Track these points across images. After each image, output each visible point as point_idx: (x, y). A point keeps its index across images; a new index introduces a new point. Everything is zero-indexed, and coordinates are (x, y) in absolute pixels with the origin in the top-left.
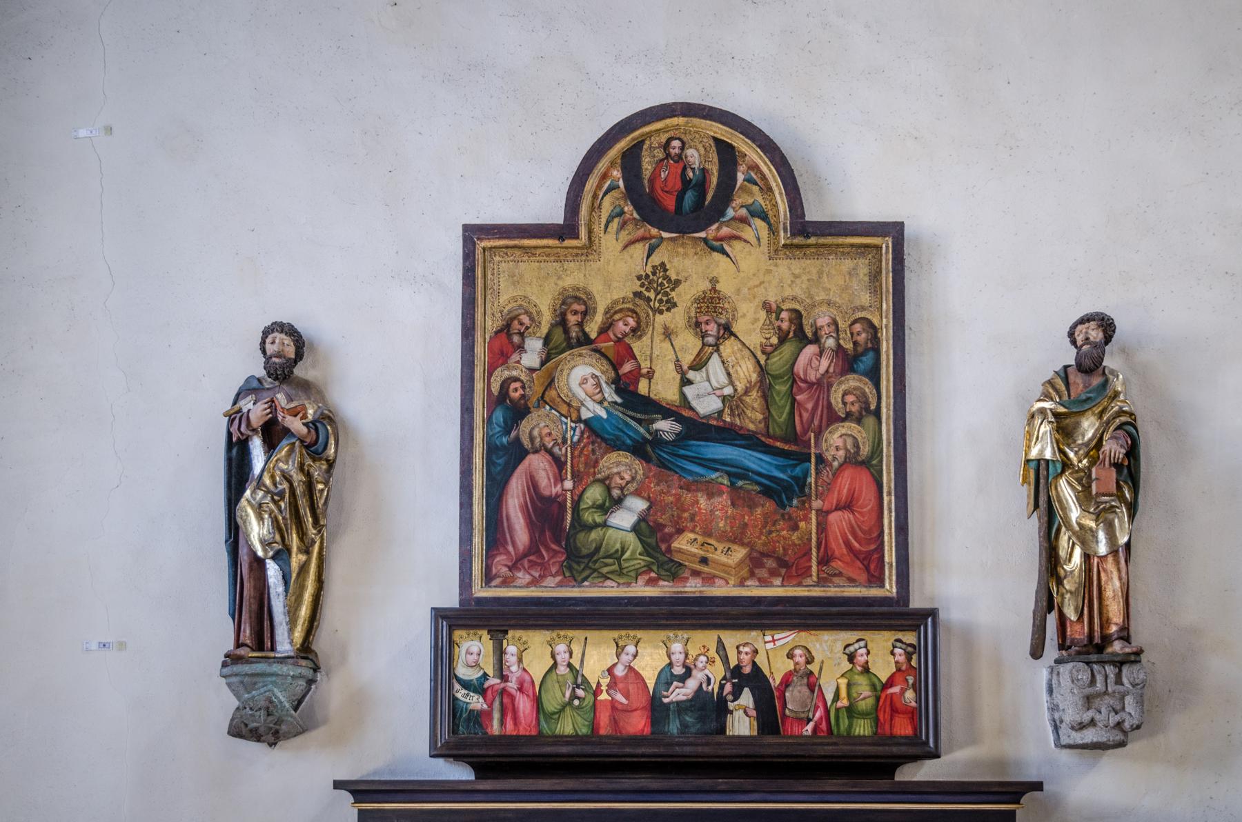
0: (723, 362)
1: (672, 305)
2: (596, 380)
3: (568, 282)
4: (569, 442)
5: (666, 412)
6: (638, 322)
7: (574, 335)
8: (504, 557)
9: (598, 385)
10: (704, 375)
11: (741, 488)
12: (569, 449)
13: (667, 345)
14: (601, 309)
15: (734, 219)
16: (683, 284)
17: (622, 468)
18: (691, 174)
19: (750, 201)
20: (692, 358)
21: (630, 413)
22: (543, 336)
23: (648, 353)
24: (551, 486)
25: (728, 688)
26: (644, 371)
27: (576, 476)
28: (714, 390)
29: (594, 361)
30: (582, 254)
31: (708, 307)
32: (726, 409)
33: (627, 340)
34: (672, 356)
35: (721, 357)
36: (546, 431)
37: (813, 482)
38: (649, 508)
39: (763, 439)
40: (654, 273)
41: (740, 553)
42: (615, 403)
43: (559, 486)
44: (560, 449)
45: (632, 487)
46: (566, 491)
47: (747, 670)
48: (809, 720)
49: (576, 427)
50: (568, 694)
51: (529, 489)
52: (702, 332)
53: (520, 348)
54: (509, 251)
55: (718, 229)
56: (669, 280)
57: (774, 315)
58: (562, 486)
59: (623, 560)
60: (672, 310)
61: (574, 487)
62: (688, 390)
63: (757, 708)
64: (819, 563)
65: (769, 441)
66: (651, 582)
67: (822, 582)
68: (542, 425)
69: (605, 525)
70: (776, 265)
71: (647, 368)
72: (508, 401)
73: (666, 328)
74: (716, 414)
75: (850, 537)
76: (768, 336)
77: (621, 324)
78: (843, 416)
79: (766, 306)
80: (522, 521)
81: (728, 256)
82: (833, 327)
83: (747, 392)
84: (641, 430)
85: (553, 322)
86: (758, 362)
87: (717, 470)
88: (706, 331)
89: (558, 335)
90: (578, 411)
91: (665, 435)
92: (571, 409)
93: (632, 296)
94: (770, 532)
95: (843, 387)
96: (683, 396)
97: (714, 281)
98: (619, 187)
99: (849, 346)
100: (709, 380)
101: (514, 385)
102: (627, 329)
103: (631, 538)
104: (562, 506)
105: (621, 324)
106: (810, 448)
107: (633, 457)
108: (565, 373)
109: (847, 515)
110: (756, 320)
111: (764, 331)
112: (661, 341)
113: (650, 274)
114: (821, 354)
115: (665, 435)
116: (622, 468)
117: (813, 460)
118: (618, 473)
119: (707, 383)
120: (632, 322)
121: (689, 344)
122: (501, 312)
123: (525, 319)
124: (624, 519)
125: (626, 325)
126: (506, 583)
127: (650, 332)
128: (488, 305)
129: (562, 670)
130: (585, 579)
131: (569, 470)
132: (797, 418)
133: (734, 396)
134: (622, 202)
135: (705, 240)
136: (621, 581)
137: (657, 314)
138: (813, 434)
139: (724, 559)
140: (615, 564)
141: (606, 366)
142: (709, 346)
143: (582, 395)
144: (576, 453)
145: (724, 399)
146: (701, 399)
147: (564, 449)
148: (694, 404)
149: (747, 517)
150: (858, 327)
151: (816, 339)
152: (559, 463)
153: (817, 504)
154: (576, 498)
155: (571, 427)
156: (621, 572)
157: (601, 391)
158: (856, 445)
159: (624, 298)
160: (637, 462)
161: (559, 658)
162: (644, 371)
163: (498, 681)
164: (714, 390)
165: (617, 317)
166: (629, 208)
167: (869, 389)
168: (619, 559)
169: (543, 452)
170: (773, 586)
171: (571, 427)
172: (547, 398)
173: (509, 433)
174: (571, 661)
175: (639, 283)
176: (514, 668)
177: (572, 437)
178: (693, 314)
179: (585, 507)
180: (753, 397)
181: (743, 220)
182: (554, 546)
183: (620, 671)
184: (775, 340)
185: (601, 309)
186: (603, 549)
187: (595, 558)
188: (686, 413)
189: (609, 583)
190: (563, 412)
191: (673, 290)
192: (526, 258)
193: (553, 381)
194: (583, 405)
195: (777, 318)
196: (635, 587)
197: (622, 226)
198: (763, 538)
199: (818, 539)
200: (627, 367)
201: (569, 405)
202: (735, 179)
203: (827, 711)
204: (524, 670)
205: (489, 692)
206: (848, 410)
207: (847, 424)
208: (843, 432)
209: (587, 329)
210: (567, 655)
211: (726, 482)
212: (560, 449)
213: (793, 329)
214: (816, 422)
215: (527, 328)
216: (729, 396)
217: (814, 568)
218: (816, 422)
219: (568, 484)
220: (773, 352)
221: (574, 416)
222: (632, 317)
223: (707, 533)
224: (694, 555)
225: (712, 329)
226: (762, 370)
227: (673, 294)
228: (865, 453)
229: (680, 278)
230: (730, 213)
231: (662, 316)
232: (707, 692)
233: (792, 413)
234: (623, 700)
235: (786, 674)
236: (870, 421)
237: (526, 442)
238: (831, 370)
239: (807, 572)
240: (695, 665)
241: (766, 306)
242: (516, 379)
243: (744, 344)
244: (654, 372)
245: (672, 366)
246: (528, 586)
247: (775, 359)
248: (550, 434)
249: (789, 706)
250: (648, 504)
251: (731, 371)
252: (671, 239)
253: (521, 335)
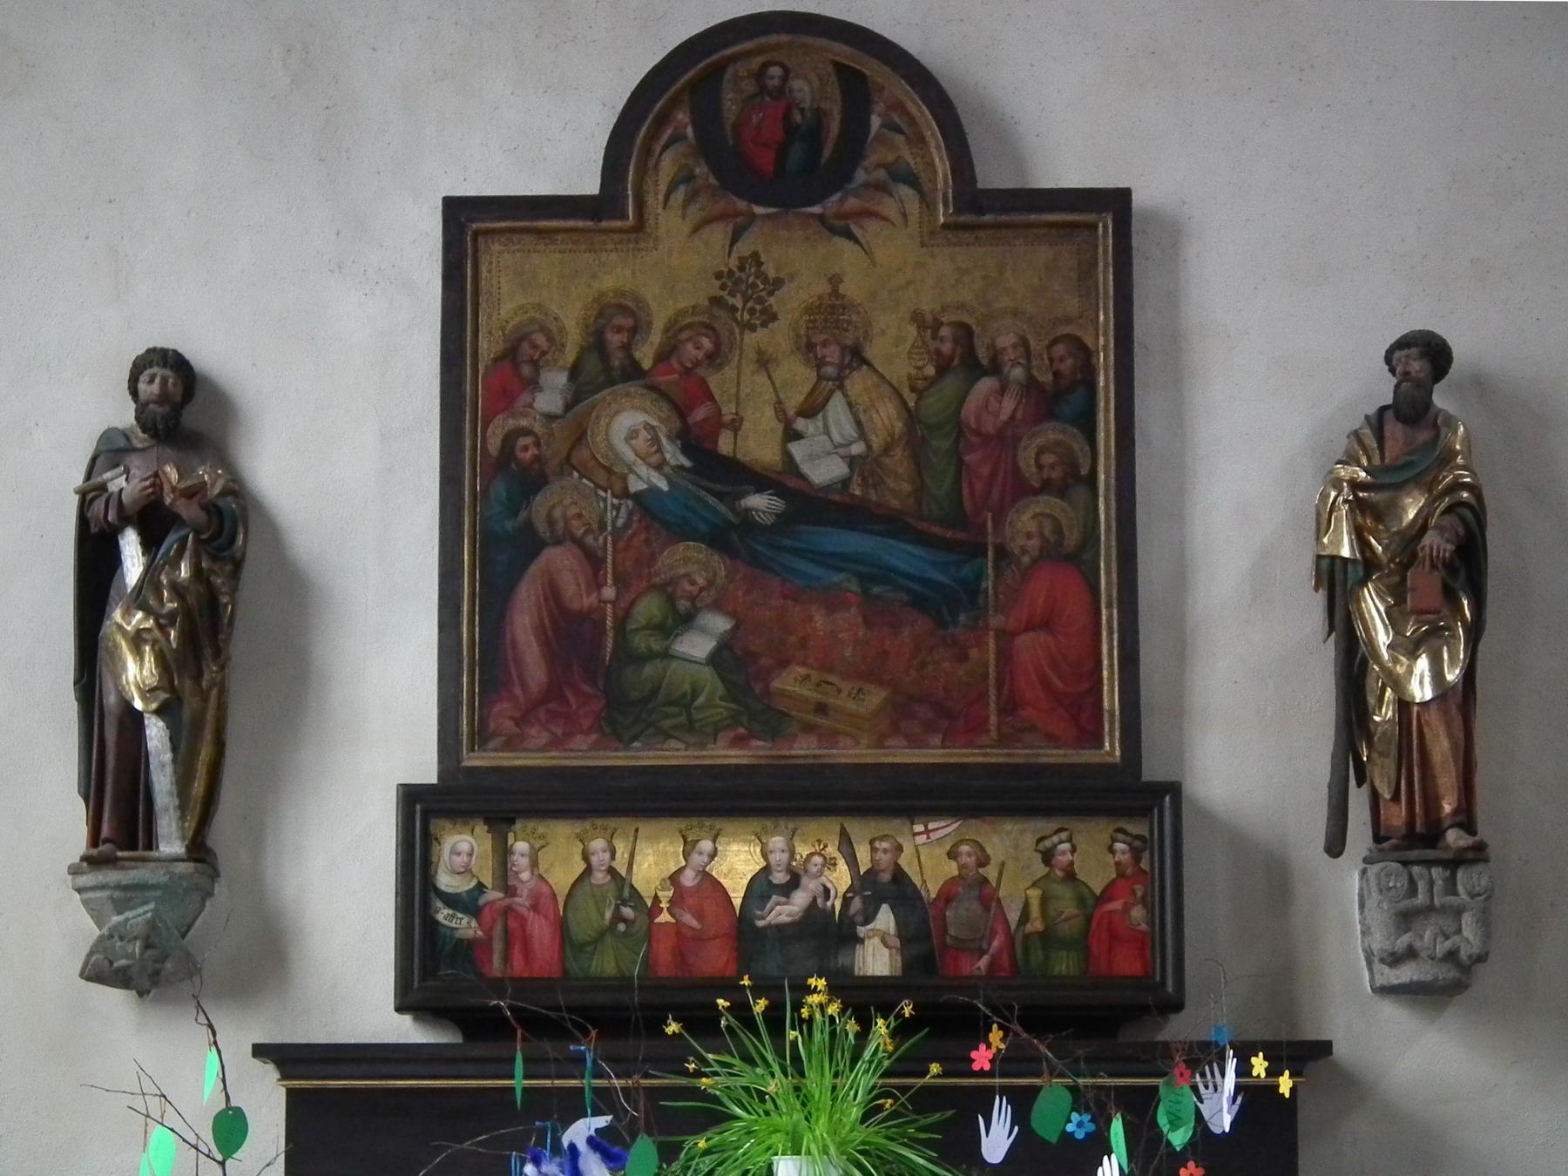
0: (850, 405)
1: (770, 317)
2: (651, 431)
3: (608, 283)
4: (609, 528)
5: (760, 481)
6: (717, 344)
7: (616, 363)
8: (506, 705)
9: (655, 440)
10: (820, 424)
11: (878, 597)
12: (609, 538)
13: (762, 379)
14: (659, 324)
15: (866, 185)
16: (787, 283)
17: (691, 568)
18: (798, 118)
19: (891, 157)
20: (802, 398)
21: (706, 483)
22: (569, 366)
23: (733, 391)
24: (581, 596)
25: (857, 904)
26: (727, 418)
27: (621, 581)
28: (835, 447)
29: (649, 403)
30: (630, 240)
31: (826, 321)
32: (856, 477)
33: (701, 372)
34: (769, 395)
35: (845, 395)
36: (573, 511)
37: (990, 588)
38: (735, 628)
39: (912, 521)
40: (741, 268)
41: (876, 697)
42: (682, 467)
43: (595, 595)
44: (596, 539)
45: (708, 597)
46: (605, 602)
47: (886, 877)
48: (982, 953)
49: (620, 504)
50: (608, 915)
51: (546, 599)
52: (816, 358)
53: (533, 385)
54: (515, 237)
55: (842, 200)
56: (766, 280)
57: (929, 332)
58: (599, 594)
59: (695, 708)
60: (770, 325)
61: (617, 597)
62: (796, 449)
63: (900, 935)
64: (1001, 712)
65: (923, 526)
66: (739, 742)
67: (1004, 740)
68: (567, 501)
69: (667, 655)
70: (932, 256)
71: (732, 413)
72: (513, 466)
73: (760, 352)
74: (839, 485)
75: (1049, 672)
76: (920, 364)
77: (690, 347)
78: (1037, 485)
79: (917, 318)
80: (535, 648)
81: (856, 241)
82: (1021, 349)
83: (887, 450)
84: (723, 508)
85: (583, 343)
86: (904, 403)
87: (840, 570)
88: (824, 357)
89: (593, 364)
90: (624, 479)
91: (759, 516)
92: (612, 476)
93: (706, 303)
94: (924, 664)
95: (1038, 441)
96: (788, 457)
97: (835, 280)
98: (685, 138)
99: (1046, 378)
100: (827, 432)
101: (522, 441)
102: (700, 355)
103: (707, 673)
104: (599, 626)
105: (690, 347)
106: (986, 536)
107: (710, 551)
108: (603, 422)
109: (1043, 637)
110: (898, 341)
111: (914, 356)
112: (753, 373)
113: (735, 270)
114: (1002, 390)
115: (759, 516)
116: (691, 568)
117: (990, 554)
118: (687, 575)
119: (826, 437)
120: (706, 343)
121: (797, 377)
122: (503, 329)
123: (540, 340)
124: (697, 646)
125: (698, 348)
126: (510, 744)
127: (736, 359)
128: (482, 319)
129: (600, 877)
130: (635, 738)
131: (609, 570)
132: (966, 492)
133: (867, 456)
134: (690, 162)
135: (821, 218)
136: (692, 740)
137: (747, 332)
138: (990, 514)
139: (851, 705)
140: (680, 715)
141: (665, 410)
142: (829, 379)
143: (629, 455)
144: (621, 544)
145: (852, 461)
146: (817, 462)
147: (601, 538)
148: (805, 468)
149: (887, 642)
150: (1060, 349)
151: (995, 368)
152: (594, 560)
153: (996, 621)
154: (620, 613)
155: (613, 505)
156: (690, 727)
157: (660, 450)
158: (1058, 529)
159: (694, 307)
160: (716, 557)
161: (594, 860)
162: (727, 418)
163: (501, 895)
164: (835, 447)
165: (683, 336)
166: (701, 170)
167: (1079, 445)
168: (688, 707)
169: (568, 543)
170: (927, 746)
171: (613, 505)
172: (574, 461)
173: (516, 514)
174: (614, 864)
175: (717, 283)
176: (525, 876)
177: (614, 521)
178: (802, 332)
179: (634, 627)
180: (896, 458)
181: (880, 187)
182: (587, 688)
183: (689, 879)
184: (930, 371)
185: (659, 324)
186: (662, 691)
187: (651, 706)
188: (792, 483)
189: (673, 743)
190: (601, 483)
191: (771, 293)
192: (541, 247)
193: (584, 433)
194: (632, 471)
195: (935, 337)
196: (713, 749)
197: (691, 198)
198: (913, 673)
199: (998, 673)
200: (700, 413)
201: (609, 471)
202: (866, 125)
203: (1010, 938)
204: (541, 878)
205: (487, 911)
206: (1045, 476)
207: (1043, 498)
208: (1037, 510)
209: (637, 355)
210: (607, 855)
211: (854, 586)
212: (596, 539)
213: (958, 353)
214: (996, 494)
215: (544, 353)
216: (860, 456)
217: (993, 719)
218: (996, 494)
219: (609, 592)
220: (927, 389)
221: (618, 488)
222: (707, 336)
223: (826, 666)
224: (806, 700)
225: (832, 354)
226: (911, 417)
227: (772, 300)
228: (1073, 543)
229: (781, 275)
230: (860, 176)
231: (754, 335)
232: (824, 911)
233: (958, 481)
234: (694, 923)
235: (946, 883)
236: (1080, 493)
237: (542, 527)
238: (1019, 415)
239: (980, 726)
240: (806, 871)
241: (917, 318)
242: (527, 432)
243: (882, 377)
244: (742, 420)
245: (769, 412)
246: (544, 749)
247: (931, 400)
248: (580, 516)
249: (952, 931)
250: (734, 622)
251: (862, 417)
252: (769, 216)
253: (536, 365)
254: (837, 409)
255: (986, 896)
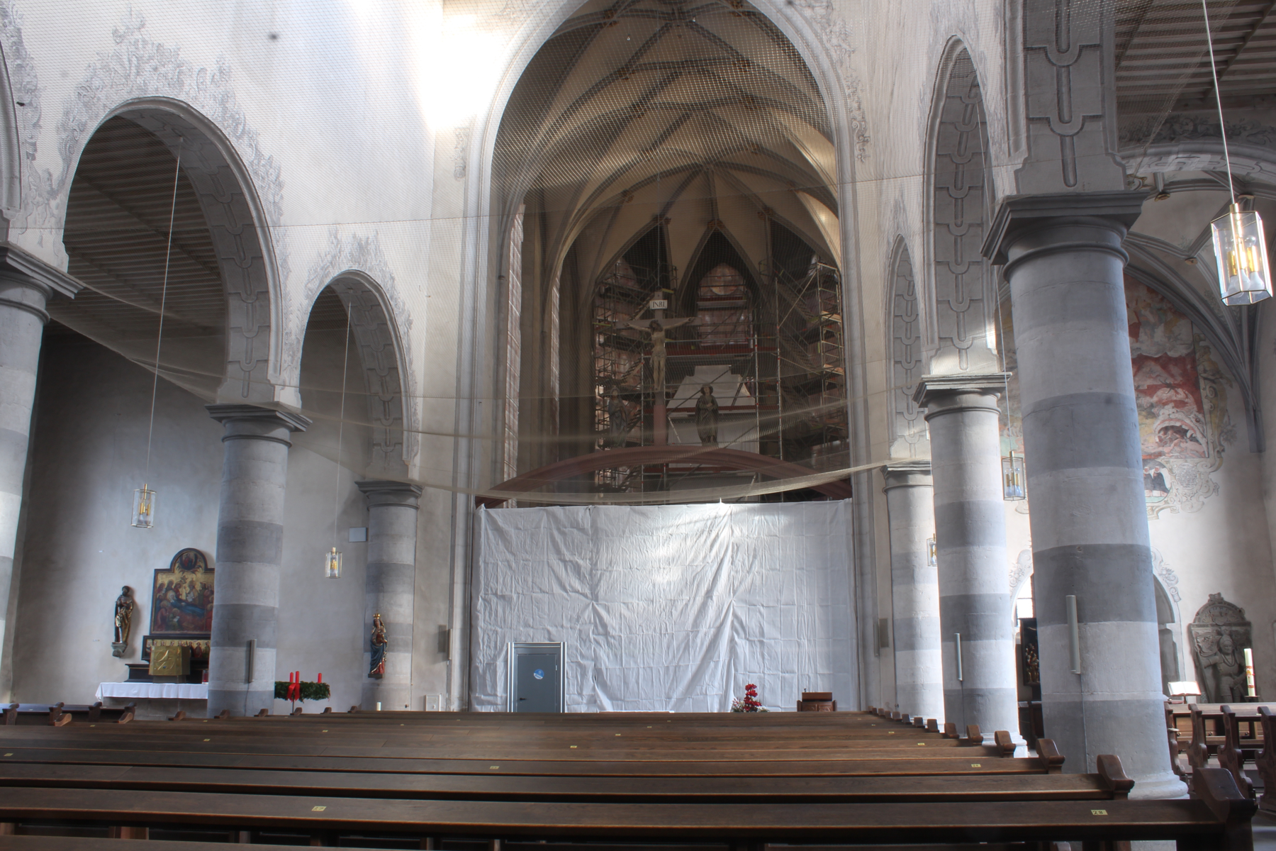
1: (186, 583)
79: (201, 583)
92: (169, 601)
124: (176, 620)
152: (166, 610)
254: (192, 593)
255: (200, 648)
